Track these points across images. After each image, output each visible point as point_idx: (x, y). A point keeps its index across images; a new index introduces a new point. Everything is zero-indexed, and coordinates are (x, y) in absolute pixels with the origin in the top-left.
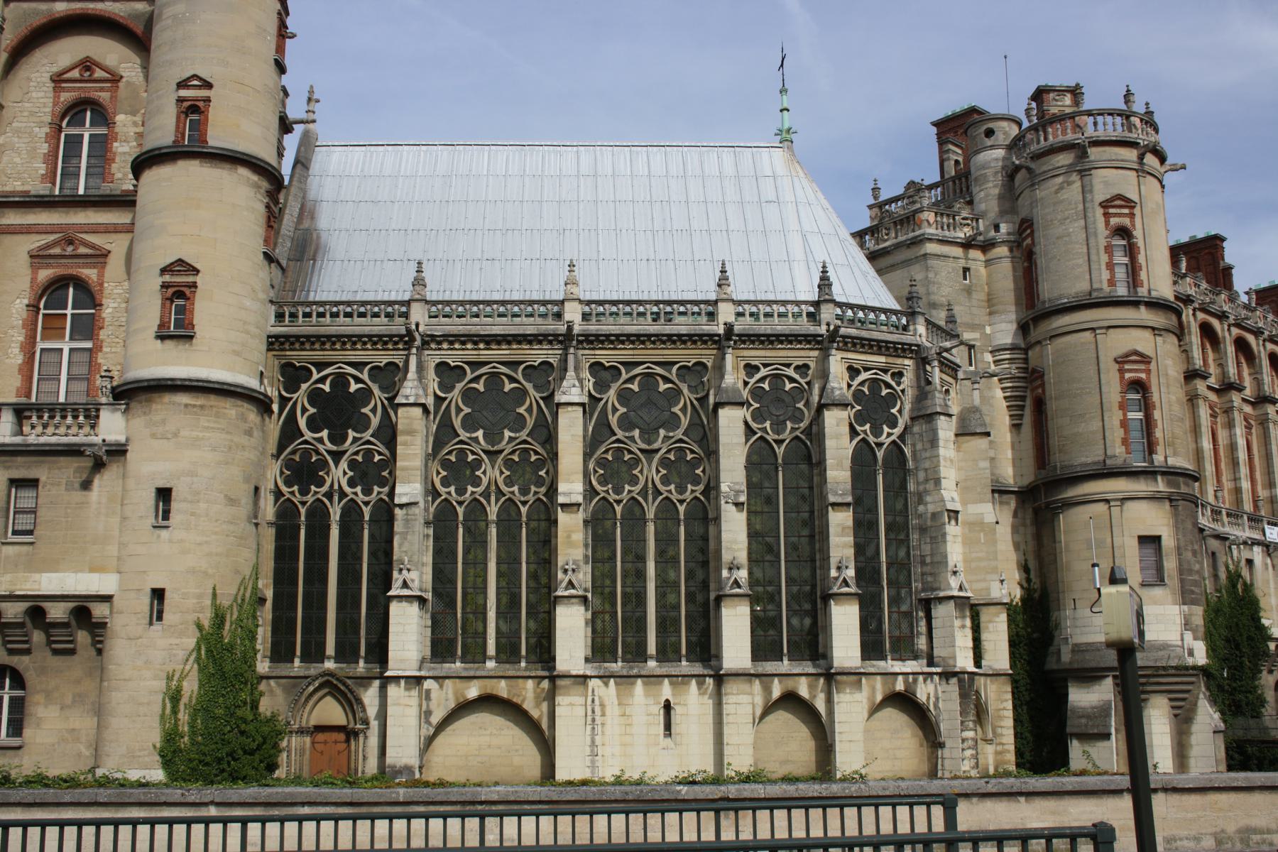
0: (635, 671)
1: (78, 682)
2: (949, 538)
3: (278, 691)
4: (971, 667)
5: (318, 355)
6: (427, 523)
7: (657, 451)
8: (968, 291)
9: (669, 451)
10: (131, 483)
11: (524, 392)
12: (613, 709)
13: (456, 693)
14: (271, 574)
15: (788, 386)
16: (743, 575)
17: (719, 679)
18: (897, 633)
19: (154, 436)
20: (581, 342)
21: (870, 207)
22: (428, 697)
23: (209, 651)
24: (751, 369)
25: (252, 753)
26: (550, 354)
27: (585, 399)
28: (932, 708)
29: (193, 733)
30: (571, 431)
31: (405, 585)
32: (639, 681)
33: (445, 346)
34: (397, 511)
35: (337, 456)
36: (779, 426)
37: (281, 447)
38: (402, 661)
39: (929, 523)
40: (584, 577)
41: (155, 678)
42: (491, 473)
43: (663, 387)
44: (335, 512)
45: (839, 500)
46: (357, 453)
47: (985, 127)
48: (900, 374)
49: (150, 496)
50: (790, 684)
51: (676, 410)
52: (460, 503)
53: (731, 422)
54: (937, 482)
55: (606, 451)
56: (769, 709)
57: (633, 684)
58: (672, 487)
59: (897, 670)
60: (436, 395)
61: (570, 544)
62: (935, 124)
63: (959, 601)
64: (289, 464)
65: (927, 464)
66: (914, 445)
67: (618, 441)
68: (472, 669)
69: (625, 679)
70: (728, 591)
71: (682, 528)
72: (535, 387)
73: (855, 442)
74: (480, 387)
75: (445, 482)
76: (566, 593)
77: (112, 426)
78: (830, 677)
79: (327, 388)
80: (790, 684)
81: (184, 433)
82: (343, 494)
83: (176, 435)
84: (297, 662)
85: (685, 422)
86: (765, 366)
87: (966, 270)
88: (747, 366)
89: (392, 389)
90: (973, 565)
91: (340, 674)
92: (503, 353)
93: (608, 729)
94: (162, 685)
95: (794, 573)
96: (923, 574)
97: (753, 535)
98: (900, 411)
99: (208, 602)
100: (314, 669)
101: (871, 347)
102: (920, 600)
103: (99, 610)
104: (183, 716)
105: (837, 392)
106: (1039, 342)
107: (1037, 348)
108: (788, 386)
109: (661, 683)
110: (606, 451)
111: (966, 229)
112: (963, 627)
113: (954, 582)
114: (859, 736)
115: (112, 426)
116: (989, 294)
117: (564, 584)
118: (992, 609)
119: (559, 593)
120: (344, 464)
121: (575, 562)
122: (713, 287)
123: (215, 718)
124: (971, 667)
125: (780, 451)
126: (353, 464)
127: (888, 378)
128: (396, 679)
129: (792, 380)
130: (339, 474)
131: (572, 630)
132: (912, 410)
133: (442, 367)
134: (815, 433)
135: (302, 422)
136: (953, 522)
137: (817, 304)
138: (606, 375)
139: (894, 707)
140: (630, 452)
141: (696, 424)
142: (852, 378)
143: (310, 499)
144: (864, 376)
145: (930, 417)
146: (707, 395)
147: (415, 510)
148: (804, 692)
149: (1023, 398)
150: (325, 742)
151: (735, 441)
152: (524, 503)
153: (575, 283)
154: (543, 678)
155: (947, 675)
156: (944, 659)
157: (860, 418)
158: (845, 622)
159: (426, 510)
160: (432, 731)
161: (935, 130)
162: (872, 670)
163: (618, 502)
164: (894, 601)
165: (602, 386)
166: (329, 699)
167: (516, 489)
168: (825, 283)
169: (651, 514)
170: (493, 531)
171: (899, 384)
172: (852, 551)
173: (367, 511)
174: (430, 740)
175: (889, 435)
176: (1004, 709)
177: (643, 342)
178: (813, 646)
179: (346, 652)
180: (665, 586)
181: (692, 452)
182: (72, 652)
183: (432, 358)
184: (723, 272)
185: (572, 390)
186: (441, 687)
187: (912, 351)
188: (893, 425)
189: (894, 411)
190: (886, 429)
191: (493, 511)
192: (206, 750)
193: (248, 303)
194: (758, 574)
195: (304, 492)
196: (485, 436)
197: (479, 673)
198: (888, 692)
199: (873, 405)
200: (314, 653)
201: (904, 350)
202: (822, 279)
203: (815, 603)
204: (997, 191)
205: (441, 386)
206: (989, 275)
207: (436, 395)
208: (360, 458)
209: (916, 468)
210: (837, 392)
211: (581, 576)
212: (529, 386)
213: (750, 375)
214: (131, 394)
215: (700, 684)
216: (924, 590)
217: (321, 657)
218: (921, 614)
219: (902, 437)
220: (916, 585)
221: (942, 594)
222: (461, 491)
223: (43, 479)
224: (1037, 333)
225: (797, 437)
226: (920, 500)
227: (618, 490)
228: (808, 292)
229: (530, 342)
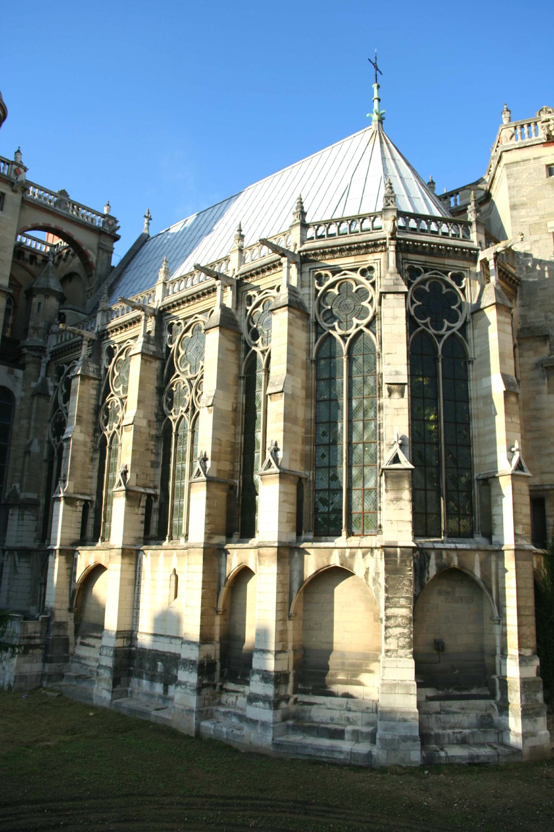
63: (390, 473)
76: (117, 489)
112: (398, 499)
136: (396, 395)
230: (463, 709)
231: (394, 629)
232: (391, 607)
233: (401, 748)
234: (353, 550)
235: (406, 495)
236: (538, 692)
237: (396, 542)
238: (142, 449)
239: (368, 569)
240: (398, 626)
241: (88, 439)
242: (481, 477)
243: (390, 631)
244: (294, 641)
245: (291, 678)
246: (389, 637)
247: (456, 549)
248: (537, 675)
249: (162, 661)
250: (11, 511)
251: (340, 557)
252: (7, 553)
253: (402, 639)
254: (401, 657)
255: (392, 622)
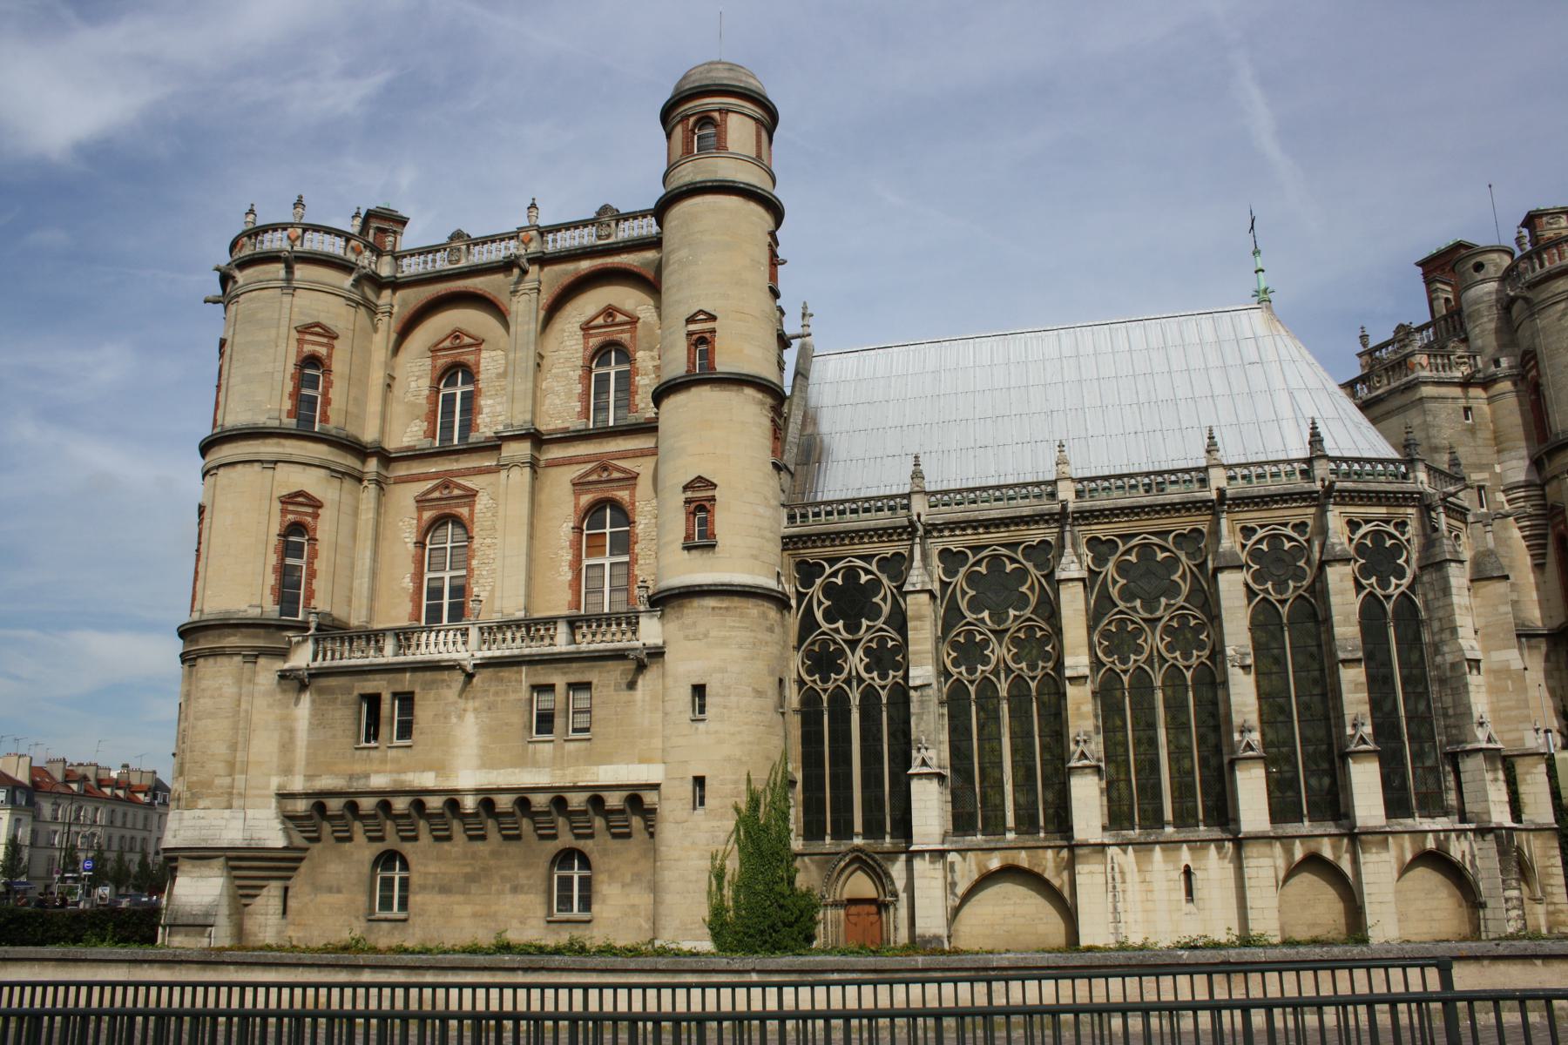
0: (1153, 838)
1: (635, 862)
2: (1471, 688)
3: (813, 868)
4: (1508, 822)
5: (829, 551)
6: (941, 703)
7: (1159, 619)
8: (1472, 430)
9: (1171, 619)
10: (670, 682)
11: (1025, 571)
12: (1133, 876)
13: (978, 865)
14: (799, 758)
15: (1287, 545)
16: (1255, 737)
17: (1239, 842)
18: (1424, 789)
19: (687, 638)
20: (1075, 519)
21: (1360, 355)
22: (952, 869)
23: (746, 832)
24: (1247, 532)
25: (791, 925)
26: (1046, 533)
27: (1085, 574)
28: (1468, 866)
29: (737, 906)
30: (1073, 606)
31: (924, 763)
32: (1157, 848)
33: (946, 533)
34: (912, 693)
35: (853, 644)
36: (1280, 586)
37: (801, 640)
38: (926, 835)
39: (1448, 674)
40: (1096, 747)
41: (701, 857)
42: (999, 651)
43: (1160, 556)
44: (855, 697)
45: (1350, 656)
46: (871, 640)
47: (1473, 262)
48: (1404, 524)
49: (687, 693)
50: (1313, 845)
51: (1176, 577)
52: (972, 682)
53: (1231, 586)
54: (1454, 631)
55: (1110, 623)
56: (1292, 871)
57: (1152, 850)
58: (1178, 654)
59: (1426, 827)
60: (941, 581)
61: (1080, 716)
62: (1419, 264)
64: (809, 654)
65: (1441, 614)
66: (1425, 595)
67: (1121, 612)
68: (993, 841)
69: (1143, 846)
70: (1241, 754)
71: (1191, 694)
72: (1036, 566)
73: (1361, 596)
74: (983, 569)
75: (956, 663)
76: (1079, 764)
77: (651, 631)
78: (1355, 838)
79: (839, 581)
80: (1313, 845)
81: (713, 633)
82: (860, 680)
83: (706, 636)
84: (828, 839)
85: (1185, 589)
86: (1262, 527)
87: (1467, 410)
88: (1244, 529)
89: (899, 577)
90: (1503, 714)
91: (869, 849)
92: (1002, 535)
93: (1129, 895)
94: (707, 864)
95: (1309, 733)
96: (1446, 727)
97: (1262, 696)
98: (1407, 561)
99: (744, 787)
100: (844, 846)
101: (1370, 499)
102: (1446, 754)
103: (649, 798)
104: (728, 892)
105: (1338, 548)
106: (1555, 477)
107: (1555, 483)
108: (1287, 545)
109: (1179, 849)
110: (1110, 623)
111: (1463, 368)
112: (1496, 780)
113: (1481, 734)
114: (1390, 897)
115: (651, 631)
116: (1495, 432)
117: (1077, 755)
118: (1528, 760)
119: (1072, 764)
120: (860, 652)
121: (1086, 733)
122: (1203, 453)
123: (756, 894)
124: (1508, 822)
125: (1284, 611)
126: (868, 651)
127: (1391, 529)
128: (921, 853)
129: (1290, 539)
130: (856, 661)
131: (1087, 800)
132: (1419, 559)
133: (945, 554)
134: (1319, 590)
135: (819, 615)
136: (1475, 672)
137: (1309, 461)
138: (1104, 549)
140: (1133, 622)
141: (1196, 590)
142: (1353, 532)
143: (830, 686)
144: (1365, 529)
145: (1440, 565)
146: (1205, 561)
147: (929, 691)
148: (1327, 853)
149: (1544, 536)
150: (858, 915)
151: (1237, 603)
152: (1033, 678)
153: (1066, 463)
154: (1062, 847)
155: (1482, 832)
156: (1477, 814)
157: (1365, 571)
158: (1365, 780)
159: (940, 690)
160: (958, 902)
161: (1420, 270)
162: (1399, 828)
163: (1125, 672)
164: (1418, 756)
165: (1100, 560)
166: (859, 873)
167: (1024, 665)
168: (1316, 439)
169: (1158, 682)
170: (1005, 707)
171: (1403, 534)
172: (1367, 708)
173: (884, 694)
174: (956, 911)
175: (1397, 586)
177: (1137, 514)
178: (1334, 804)
179: (873, 829)
180: (1179, 753)
181: (1195, 617)
182: (628, 836)
183: (935, 546)
184: (1211, 438)
185: (1071, 567)
186: (964, 859)
187: (1414, 499)
188: (1401, 575)
189: (1400, 561)
190: (1394, 581)
191: (1003, 688)
192: (749, 923)
193: (761, 510)
194: (1271, 736)
195: (825, 680)
196: (991, 616)
197: (1000, 845)
199: (1377, 558)
200: (843, 830)
201: (1405, 499)
202: (1312, 435)
203: (1332, 761)
204: (1492, 325)
205: (947, 572)
206: (1494, 412)
207: (941, 581)
208: (874, 645)
209: (1430, 619)
210: (1338, 548)
211: (1093, 746)
212: (1029, 565)
213: (1247, 537)
214: (666, 601)
215: (1220, 849)
216: (1449, 743)
217: (850, 834)
218: (1448, 768)
219: (1411, 587)
220: (1440, 739)
221: (1469, 747)
222: (972, 671)
223: (595, 682)
224: (1551, 468)
225: (1300, 596)
226: (1437, 648)
227: (1124, 661)
228: (1300, 450)
229: (1027, 523)
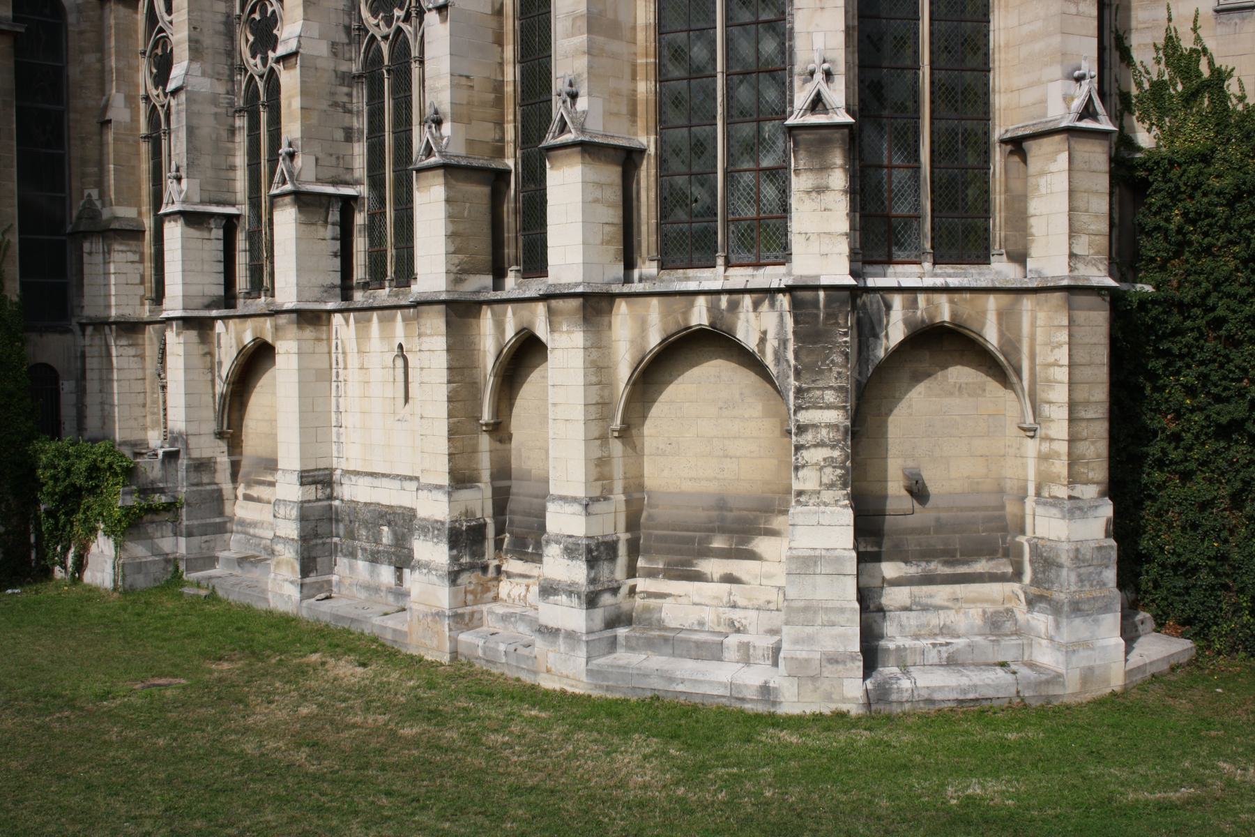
28: (769, 360)
63: (804, 136)
112: (820, 190)
139: (720, 357)
176: (1056, 364)
198: (673, 328)
230: (957, 600)
231: (812, 450)
232: (807, 408)
233: (826, 674)
234: (735, 297)
235: (838, 179)
236: (1107, 567)
237: (818, 277)
238: (324, 105)
239: (765, 333)
240: (821, 444)
241: (221, 89)
242: (1009, 135)
243: (805, 453)
244: (625, 478)
245: (622, 549)
246: (803, 466)
247: (946, 290)
248: (1107, 535)
249: (389, 524)
250: (86, 246)
251: (709, 310)
252: (89, 330)
253: (829, 470)
254: (826, 505)
255: (808, 437)
